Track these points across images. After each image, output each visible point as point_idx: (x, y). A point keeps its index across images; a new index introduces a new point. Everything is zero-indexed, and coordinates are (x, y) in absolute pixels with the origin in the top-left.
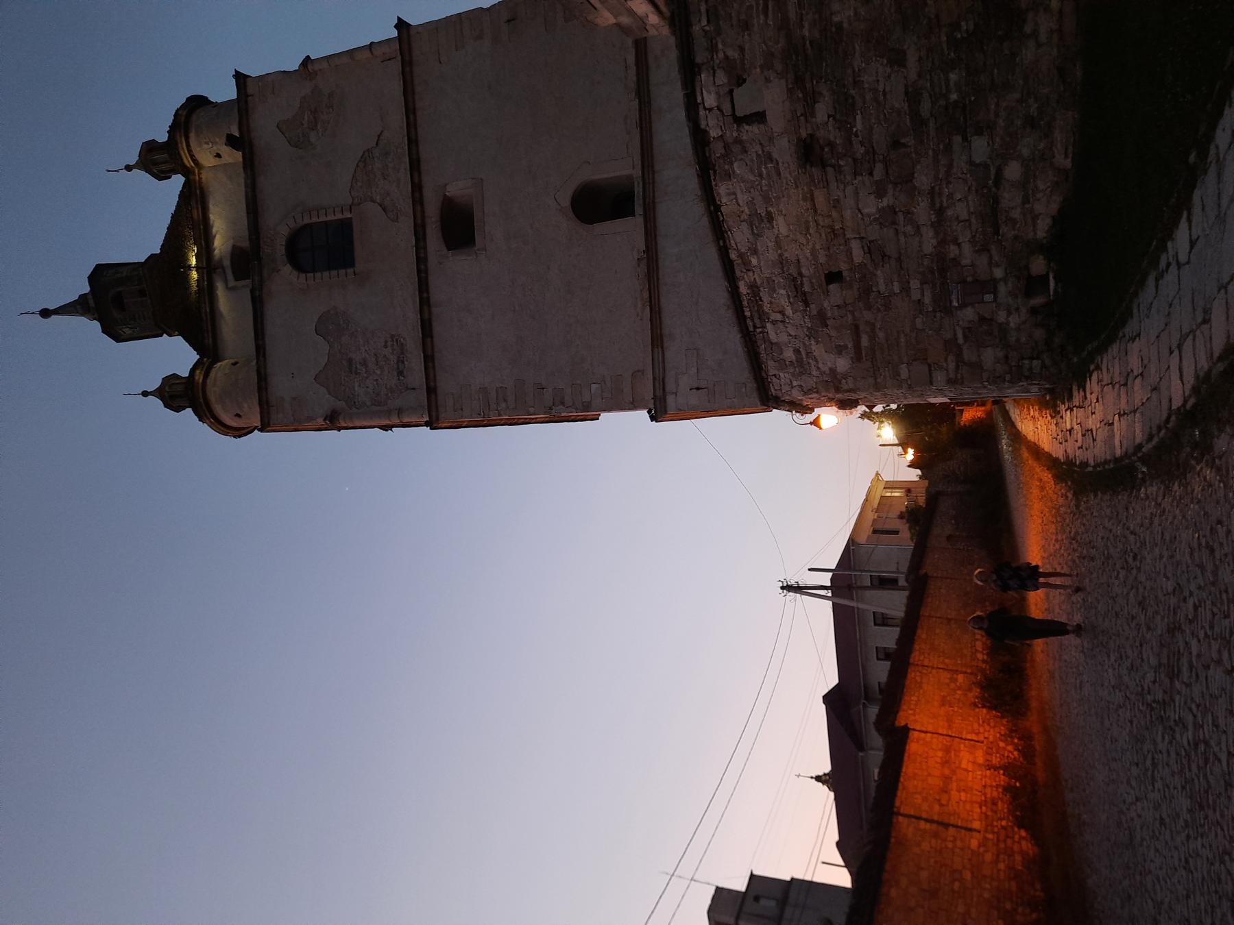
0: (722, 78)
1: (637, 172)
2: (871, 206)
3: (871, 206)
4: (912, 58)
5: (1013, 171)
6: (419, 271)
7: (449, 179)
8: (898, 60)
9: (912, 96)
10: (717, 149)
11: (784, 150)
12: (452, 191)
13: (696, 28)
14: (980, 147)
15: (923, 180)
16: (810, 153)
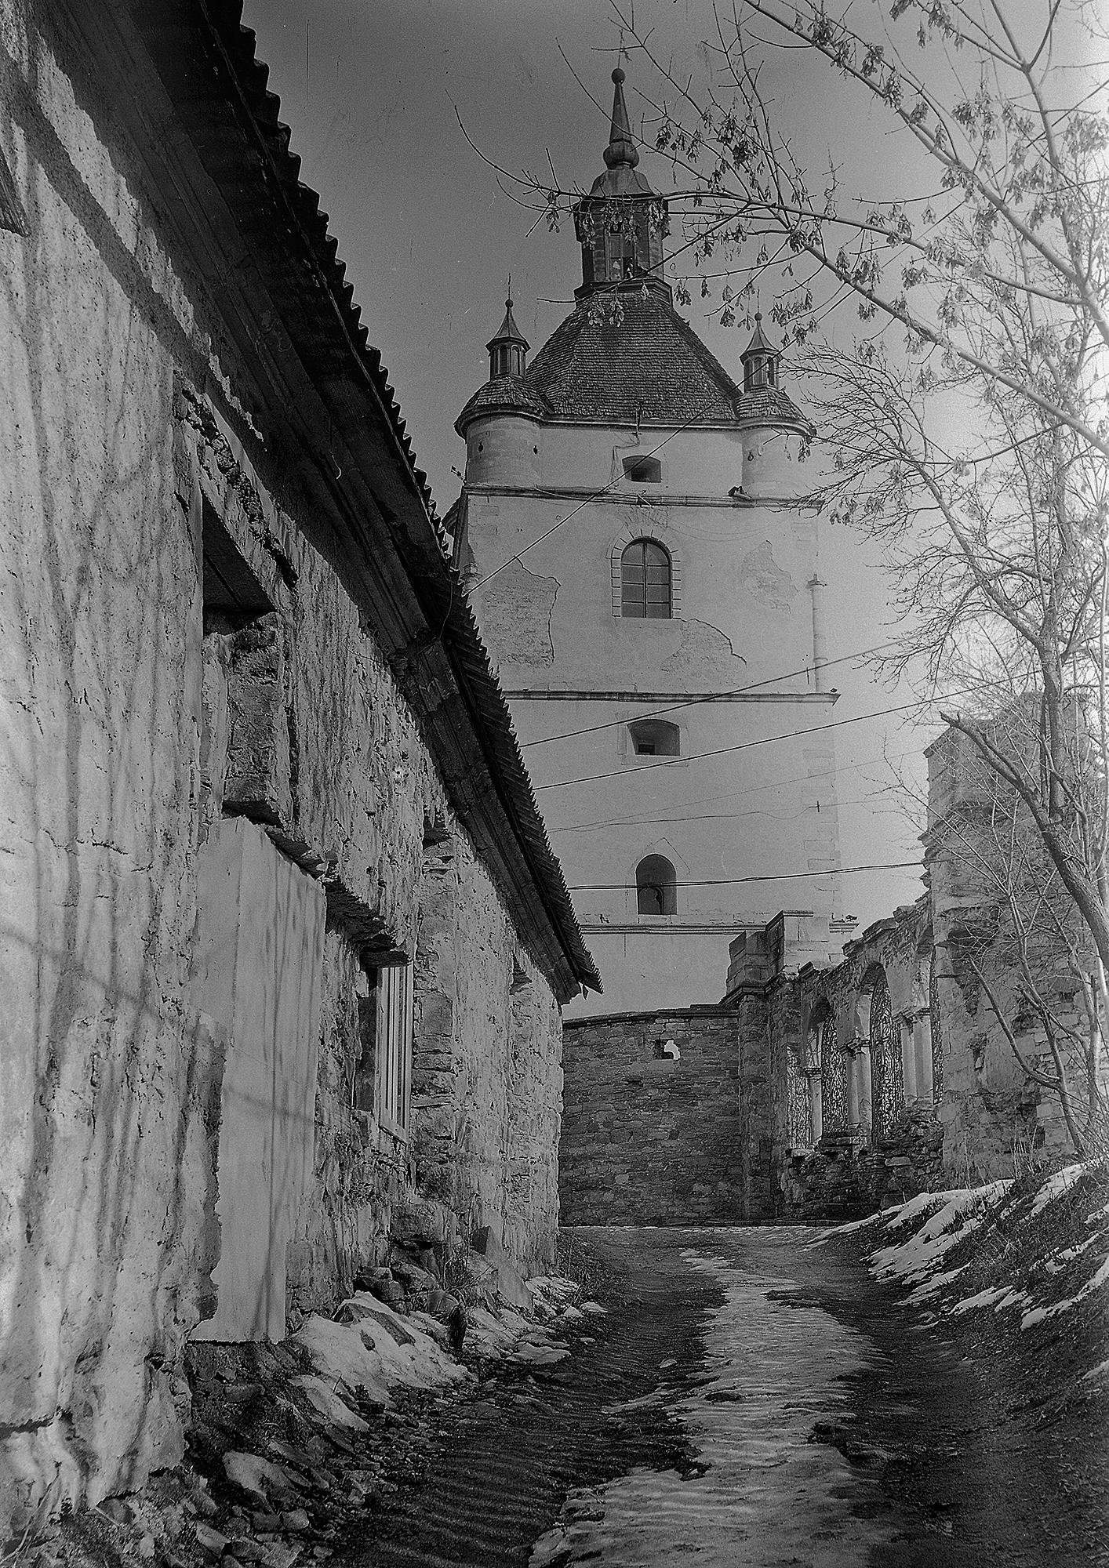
0: (680, 1034)
1: (675, 920)
2: (599, 1119)
3: (599, 1119)
4: (673, 1143)
5: (608, 1196)
6: (610, 694)
7: (696, 727)
8: (673, 1136)
9: (654, 1143)
10: (642, 1027)
11: (635, 1069)
12: (682, 732)
13: (709, 1021)
14: (622, 1179)
15: (610, 1148)
16: (635, 1082)
